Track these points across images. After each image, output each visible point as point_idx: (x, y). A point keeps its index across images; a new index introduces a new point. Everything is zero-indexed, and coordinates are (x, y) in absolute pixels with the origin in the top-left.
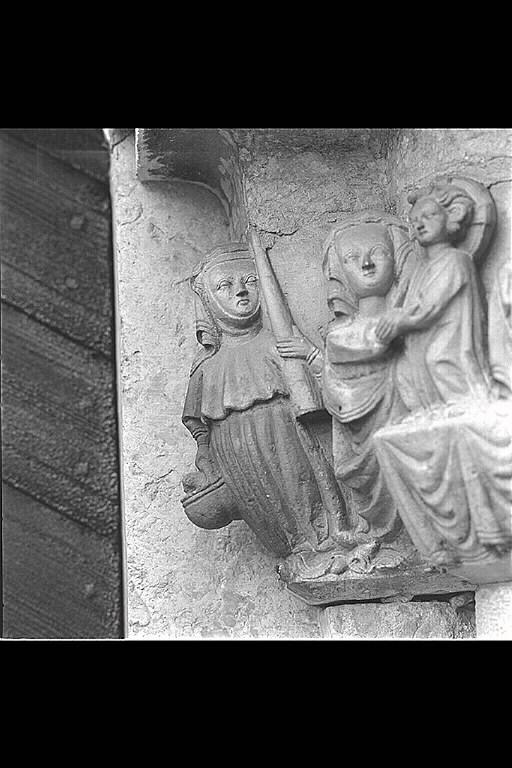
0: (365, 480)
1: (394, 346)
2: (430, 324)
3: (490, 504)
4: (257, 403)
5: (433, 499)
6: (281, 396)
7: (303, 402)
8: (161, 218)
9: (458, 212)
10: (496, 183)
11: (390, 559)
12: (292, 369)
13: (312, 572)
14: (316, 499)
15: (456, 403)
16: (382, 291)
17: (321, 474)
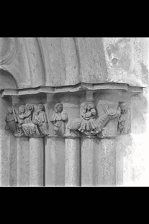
0: (21, 128)
1: (25, 118)
2: (28, 117)
3: (32, 132)
4: (12, 121)
5: (27, 131)
6: (14, 120)
7: (16, 121)
8: (3, 101)
9: (31, 108)
11: (22, 134)
12: (15, 118)
13: (16, 135)
14: (17, 129)
15: (29, 123)
16: (24, 113)
17: (17, 127)
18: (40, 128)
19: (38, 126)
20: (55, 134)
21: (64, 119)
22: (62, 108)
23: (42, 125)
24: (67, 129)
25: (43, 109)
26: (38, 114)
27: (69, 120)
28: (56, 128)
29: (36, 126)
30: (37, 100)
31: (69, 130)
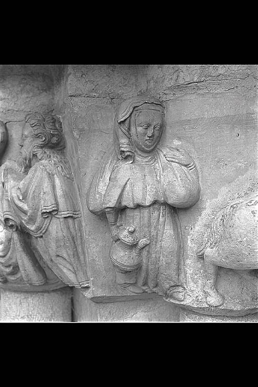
10: (9, 122)
18: (40, 245)
19: (23, 233)
20: (125, 286)
21: (178, 192)
22: (162, 128)
23: (44, 234)
24: (190, 266)
25: (54, 140)
26: (28, 167)
27: (208, 206)
28: (123, 257)
29: (15, 236)
30: (24, 95)
31: (211, 270)
